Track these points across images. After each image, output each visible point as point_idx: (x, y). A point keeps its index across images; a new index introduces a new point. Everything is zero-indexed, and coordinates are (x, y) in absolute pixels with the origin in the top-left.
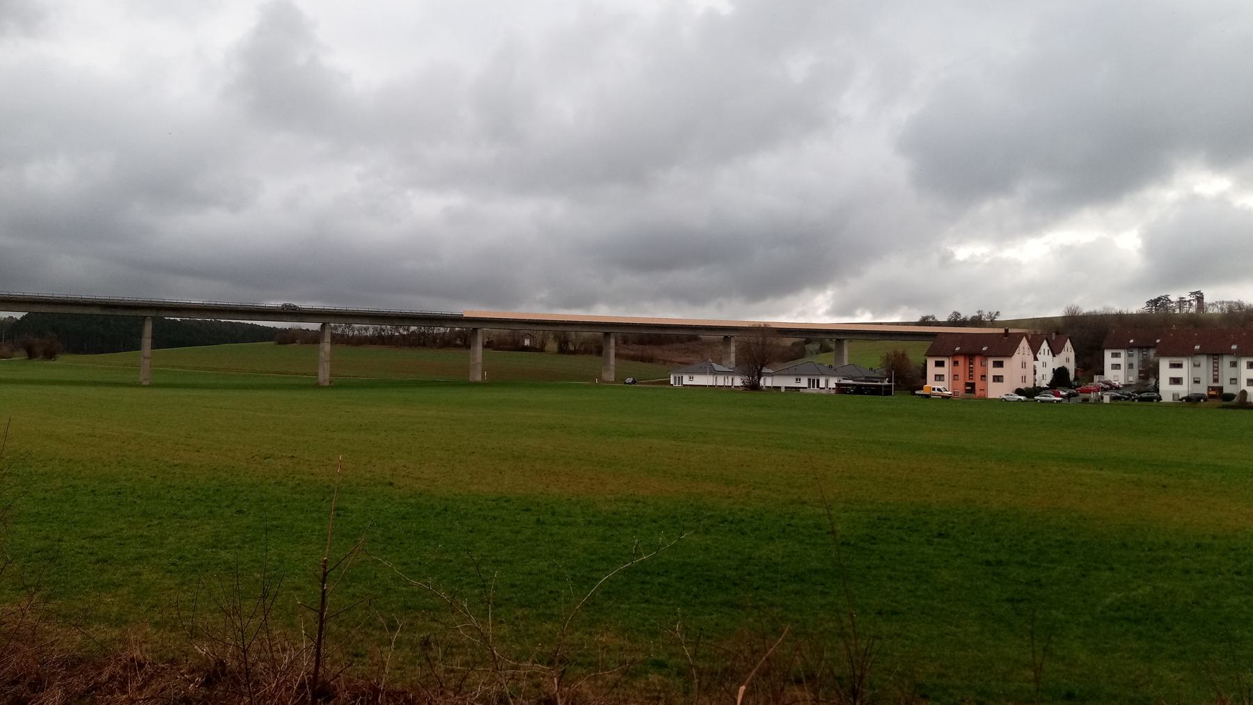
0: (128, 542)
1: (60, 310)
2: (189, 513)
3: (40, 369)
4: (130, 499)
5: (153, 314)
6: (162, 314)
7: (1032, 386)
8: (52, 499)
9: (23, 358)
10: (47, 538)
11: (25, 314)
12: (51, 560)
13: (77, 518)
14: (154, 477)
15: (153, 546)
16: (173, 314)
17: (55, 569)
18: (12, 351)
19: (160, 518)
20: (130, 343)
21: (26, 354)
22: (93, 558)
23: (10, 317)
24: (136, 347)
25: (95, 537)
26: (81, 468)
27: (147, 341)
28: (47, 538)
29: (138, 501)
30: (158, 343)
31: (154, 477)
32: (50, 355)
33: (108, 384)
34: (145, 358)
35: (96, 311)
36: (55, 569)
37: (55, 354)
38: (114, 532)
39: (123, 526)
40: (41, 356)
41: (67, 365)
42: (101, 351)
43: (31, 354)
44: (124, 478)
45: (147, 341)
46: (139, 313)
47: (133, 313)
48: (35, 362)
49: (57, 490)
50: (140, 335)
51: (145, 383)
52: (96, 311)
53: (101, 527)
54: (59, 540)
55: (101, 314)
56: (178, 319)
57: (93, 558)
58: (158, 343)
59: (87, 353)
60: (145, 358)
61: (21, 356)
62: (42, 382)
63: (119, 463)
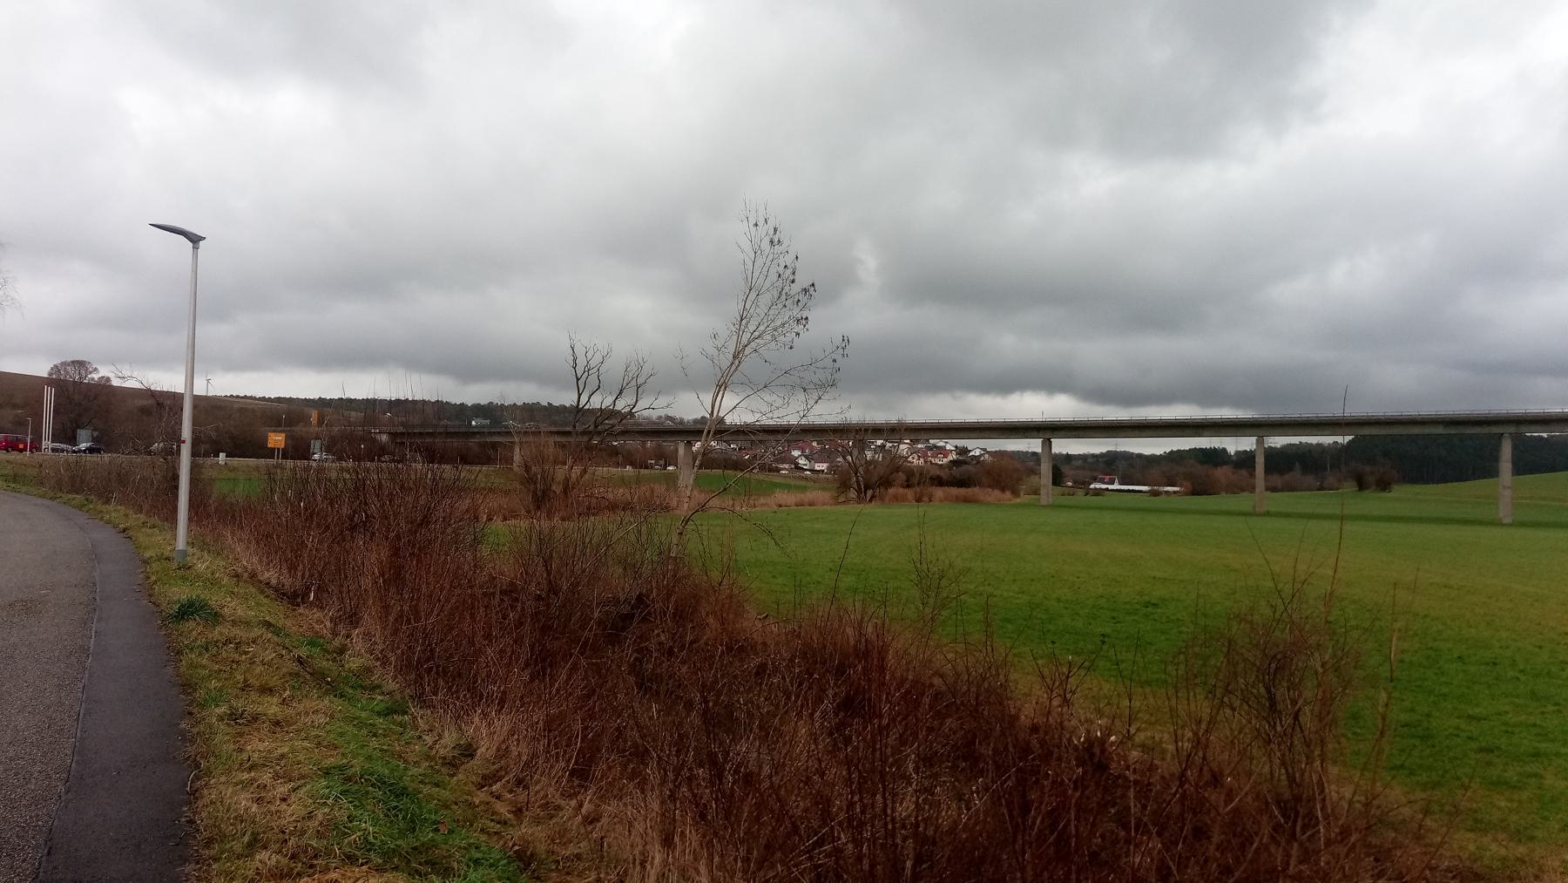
0: (1517, 730)
1: (1416, 430)
2: (256, 632)
3: (1374, 502)
4: (1511, 673)
5: (1512, 429)
6: (1523, 429)
7: (575, 404)
8: (1411, 662)
9: (1354, 489)
10: (1412, 710)
11: (1351, 437)
12: (1422, 738)
13: (1445, 690)
14: (1540, 647)
15: (1552, 741)
16: (1538, 427)
17: (1428, 751)
18: (1339, 481)
19: (1557, 704)
20: (1487, 470)
21: (1355, 484)
22: (1474, 745)
23: (1334, 442)
24: (1490, 471)
25: (1470, 718)
26: (1441, 627)
27: (1506, 465)
28: (1412, 710)
29: (1523, 678)
30: (1520, 468)
31: (1540, 647)
32: (1384, 485)
33: (1301, 516)
34: (1504, 487)
35: (1440, 430)
36: (1428, 751)
37: (1389, 484)
38: (1496, 714)
39: (1507, 708)
40: (1374, 488)
41: (1405, 497)
42: (1444, 480)
43: (1362, 485)
44: (1498, 645)
45: (1506, 465)
46: (1495, 430)
47: (1486, 430)
48: (1366, 493)
49: (1416, 652)
50: (1496, 459)
51: (1506, 521)
52: (1440, 430)
53: (1477, 705)
54: (1428, 715)
55: (1444, 432)
56: (1545, 435)
57: (1474, 745)
58: (1520, 468)
59: (1427, 482)
60: (1504, 487)
61: (1349, 487)
62: (1379, 519)
63: (1488, 624)
